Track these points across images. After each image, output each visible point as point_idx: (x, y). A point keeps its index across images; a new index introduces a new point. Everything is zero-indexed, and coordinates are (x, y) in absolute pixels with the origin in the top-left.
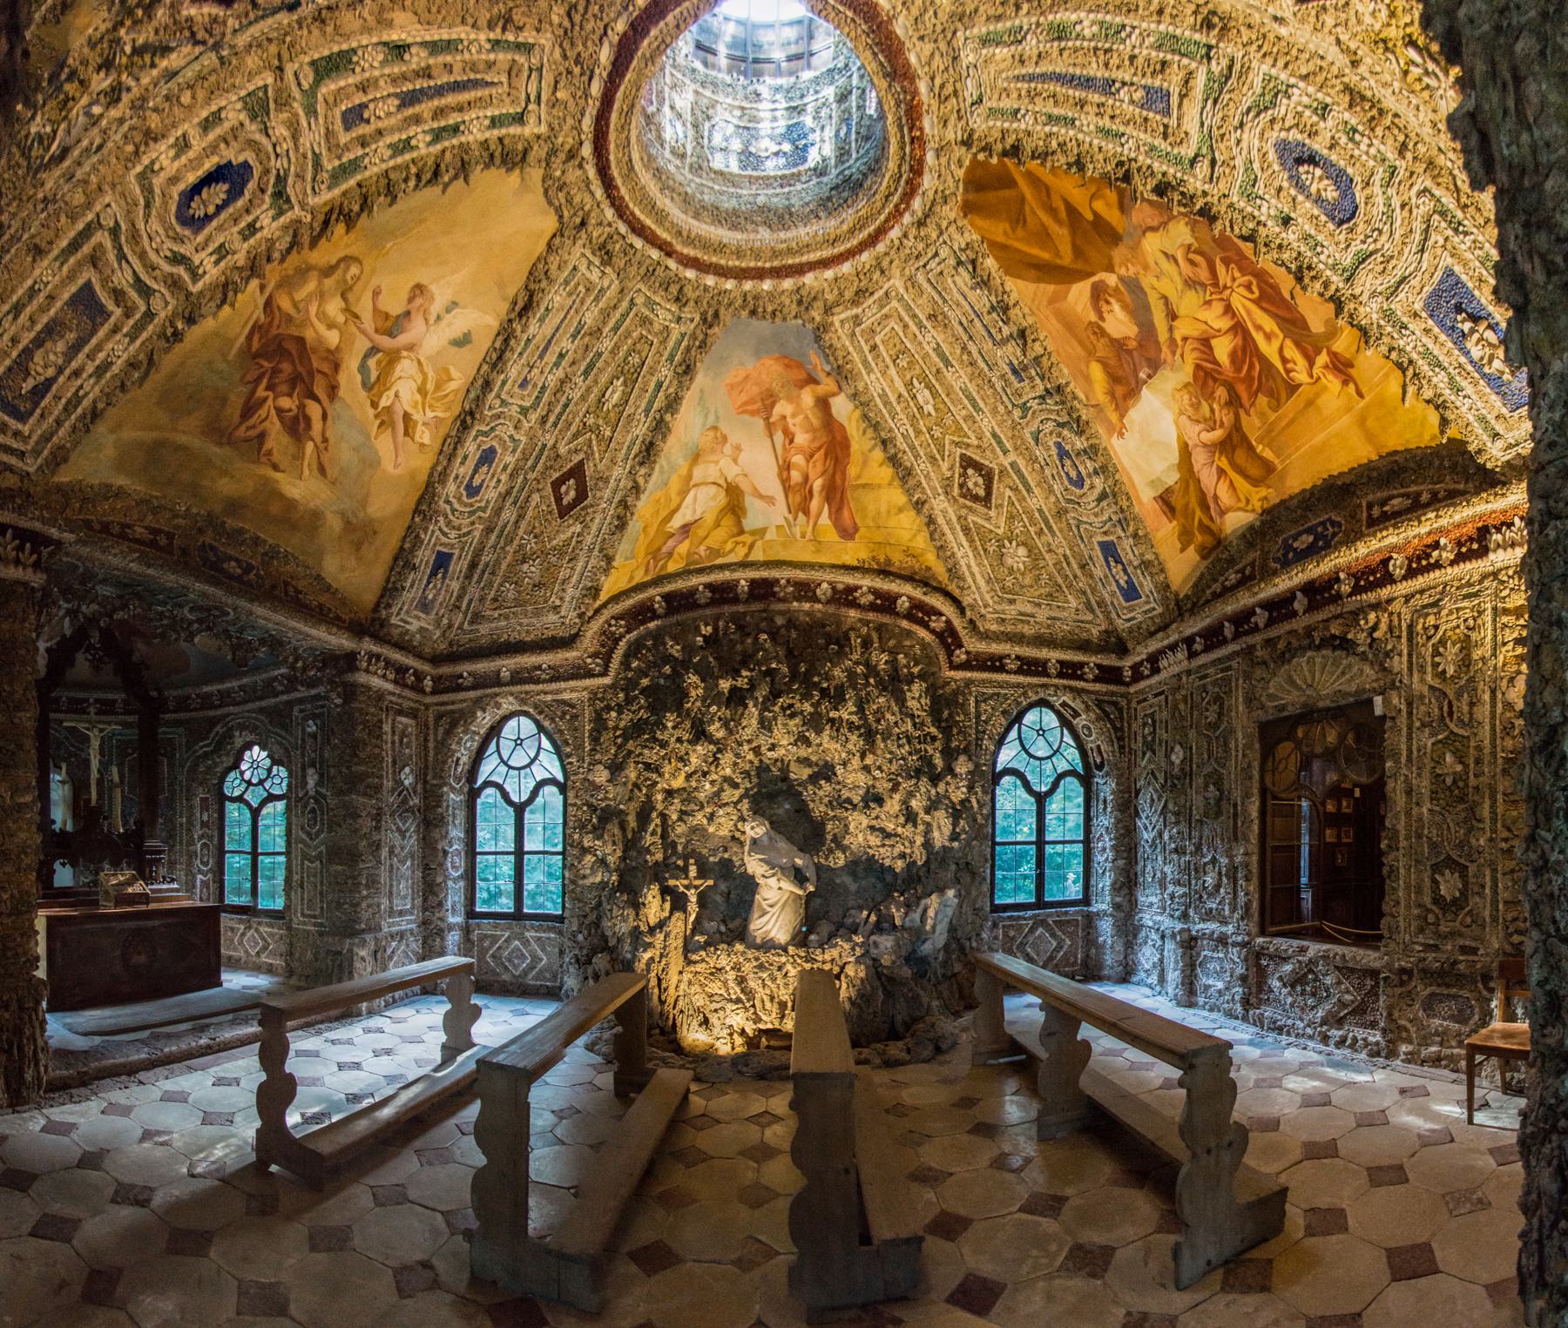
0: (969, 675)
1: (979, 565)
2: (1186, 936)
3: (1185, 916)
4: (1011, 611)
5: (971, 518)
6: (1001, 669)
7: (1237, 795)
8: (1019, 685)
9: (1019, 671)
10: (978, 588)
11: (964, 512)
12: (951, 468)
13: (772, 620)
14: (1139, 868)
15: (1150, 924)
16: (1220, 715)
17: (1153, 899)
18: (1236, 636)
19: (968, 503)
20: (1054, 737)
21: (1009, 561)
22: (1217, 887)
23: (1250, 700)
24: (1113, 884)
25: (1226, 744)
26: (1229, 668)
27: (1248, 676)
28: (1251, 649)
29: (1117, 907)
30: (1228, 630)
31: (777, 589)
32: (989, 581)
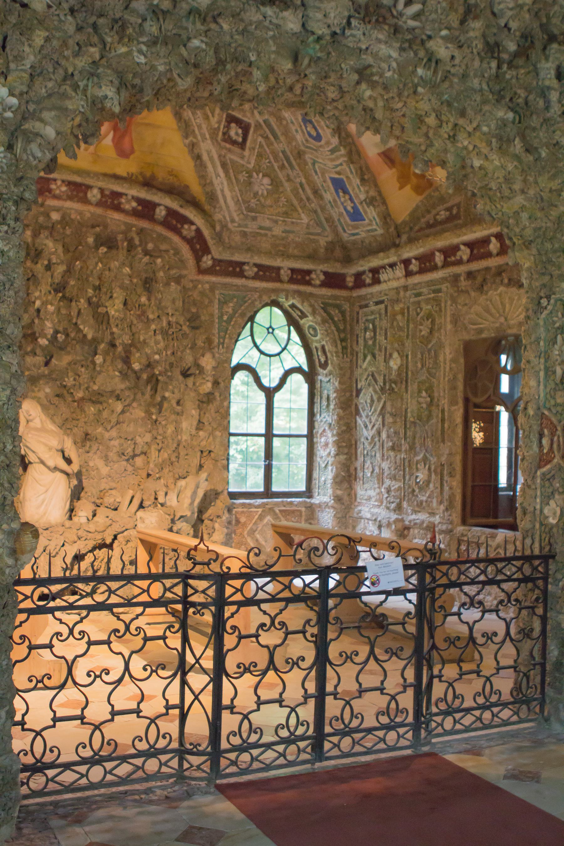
0: (213, 279)
1: (231, 191)
2: (400, 525)
3: (399, 508)
4: (252, 227)
5: (230, 156)
6: (241, 275)
7: (445, 402)
8: (255, 290)
9: (256, 277)
10: (227, 207)
11: (223, 152)
12: (219, 122)
13: (48, 216)
14: (358, 464)
15: (369, 516)
16: (431, 332)
17: (372, 493)
18: (446, 264)
19: (228, 146)
20: (282, 335)
21: (256, 188)
22: (428, 482)
23: (455, 321)
24: (335, 478)
25: (436, 356)
26: (439, 291)
27: (454, 300)
28: (456, 278)
29: (338, 499)
30: (439, 258)
31: (53, 186)
32: (237, 202)
